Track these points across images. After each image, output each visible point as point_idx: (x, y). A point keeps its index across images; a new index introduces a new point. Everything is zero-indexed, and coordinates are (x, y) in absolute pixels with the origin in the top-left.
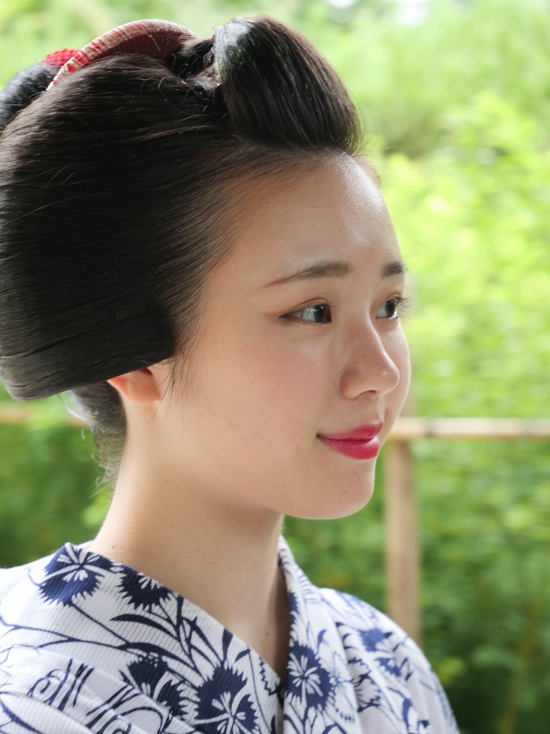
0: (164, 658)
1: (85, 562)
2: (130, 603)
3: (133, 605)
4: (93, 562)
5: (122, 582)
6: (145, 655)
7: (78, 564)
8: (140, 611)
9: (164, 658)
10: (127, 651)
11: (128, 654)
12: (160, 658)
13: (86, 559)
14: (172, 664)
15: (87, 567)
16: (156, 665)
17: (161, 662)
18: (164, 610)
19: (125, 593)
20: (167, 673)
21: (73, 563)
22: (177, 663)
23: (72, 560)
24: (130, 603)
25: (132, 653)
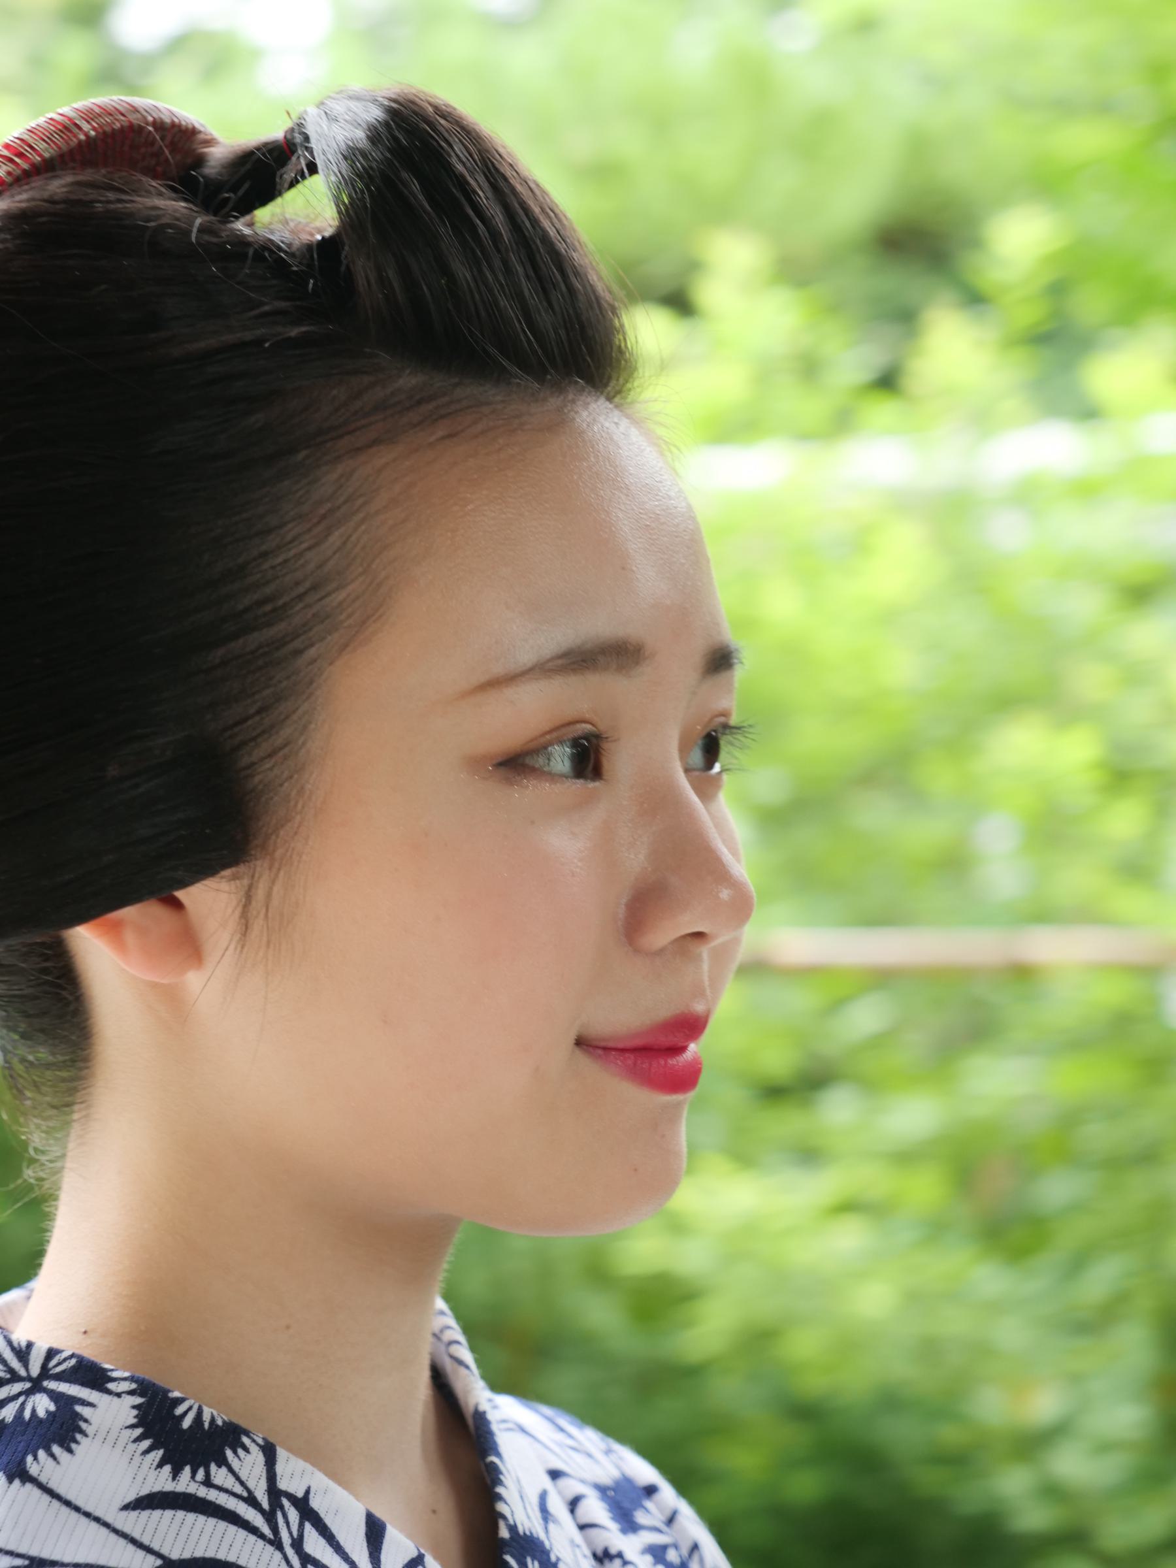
1: (45, 1373)
2: (160, 1465)
3: (167, 1468)
4: (64, 1371)
5: (136, 1417)
7: (29, 1378)
8: (186, 1483)
13: (44, 1367)
15: (52, 1385)
18: (238, 1478)
19: (146, 1443)
21: (15, 1377)
23: (11, 1371)
24: (160, 1465)
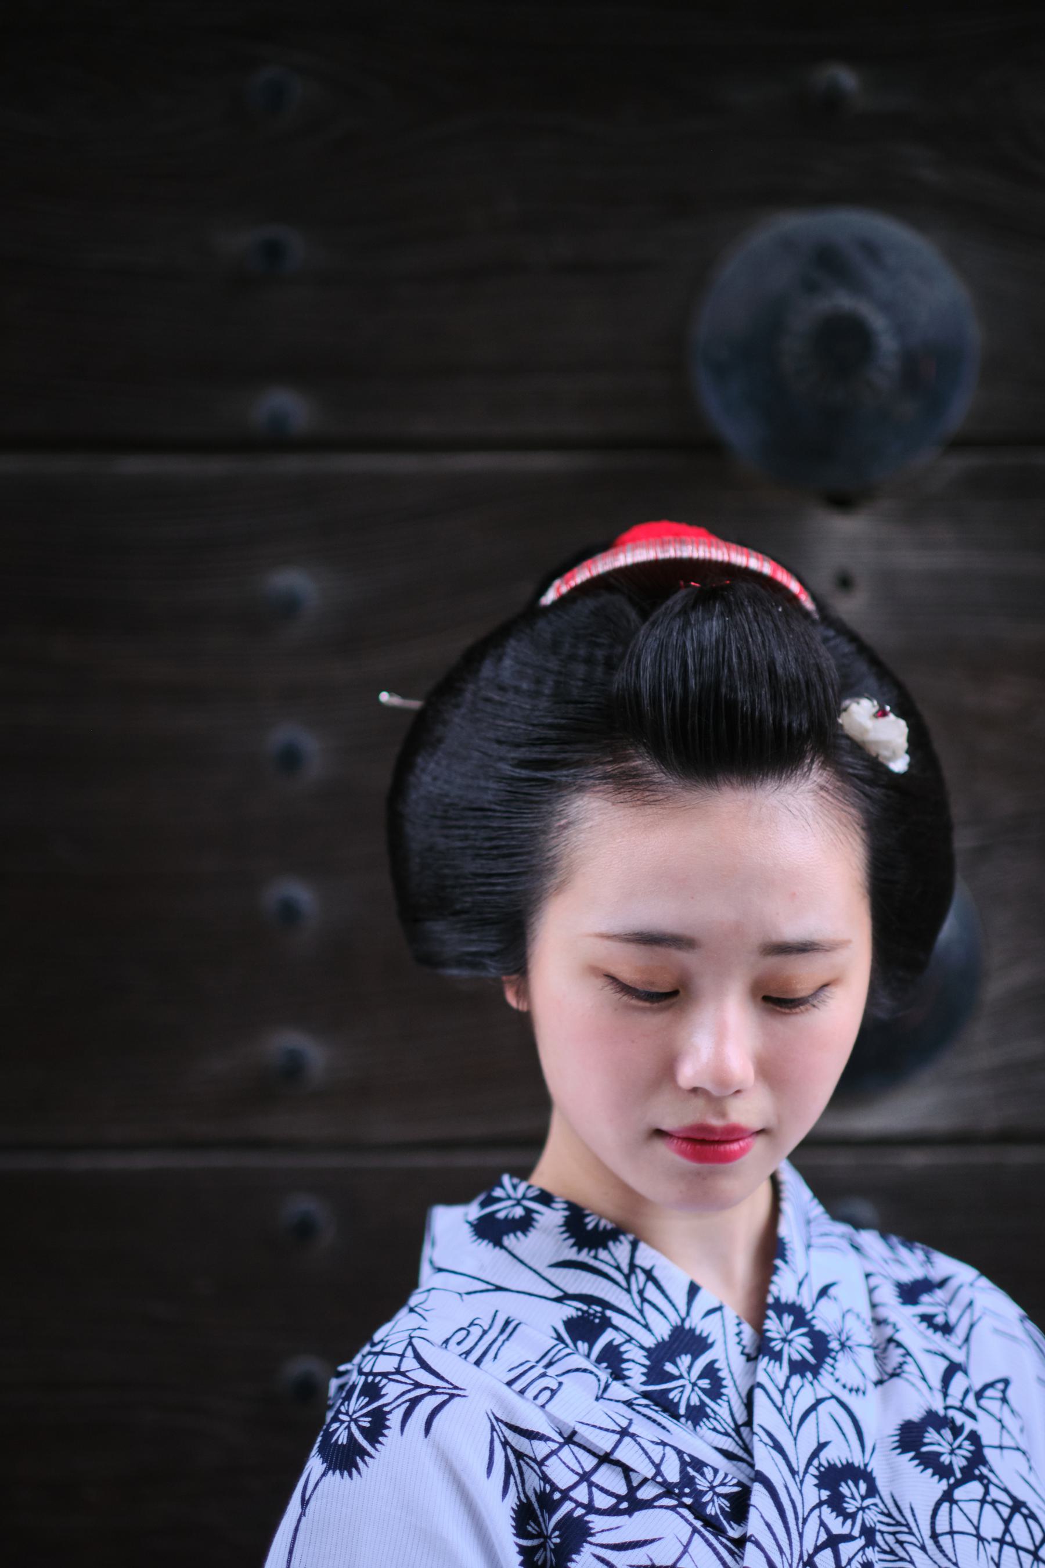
0: (609, 1313)
6: (585, 1308)
9: (609, 1313)
10: (564, 1304)
11: (565, 1307)
12: (603, 1313)
14: (616, 1319)
16: (597, 1321)
22: (624, 1318)
25: (569, 1306)
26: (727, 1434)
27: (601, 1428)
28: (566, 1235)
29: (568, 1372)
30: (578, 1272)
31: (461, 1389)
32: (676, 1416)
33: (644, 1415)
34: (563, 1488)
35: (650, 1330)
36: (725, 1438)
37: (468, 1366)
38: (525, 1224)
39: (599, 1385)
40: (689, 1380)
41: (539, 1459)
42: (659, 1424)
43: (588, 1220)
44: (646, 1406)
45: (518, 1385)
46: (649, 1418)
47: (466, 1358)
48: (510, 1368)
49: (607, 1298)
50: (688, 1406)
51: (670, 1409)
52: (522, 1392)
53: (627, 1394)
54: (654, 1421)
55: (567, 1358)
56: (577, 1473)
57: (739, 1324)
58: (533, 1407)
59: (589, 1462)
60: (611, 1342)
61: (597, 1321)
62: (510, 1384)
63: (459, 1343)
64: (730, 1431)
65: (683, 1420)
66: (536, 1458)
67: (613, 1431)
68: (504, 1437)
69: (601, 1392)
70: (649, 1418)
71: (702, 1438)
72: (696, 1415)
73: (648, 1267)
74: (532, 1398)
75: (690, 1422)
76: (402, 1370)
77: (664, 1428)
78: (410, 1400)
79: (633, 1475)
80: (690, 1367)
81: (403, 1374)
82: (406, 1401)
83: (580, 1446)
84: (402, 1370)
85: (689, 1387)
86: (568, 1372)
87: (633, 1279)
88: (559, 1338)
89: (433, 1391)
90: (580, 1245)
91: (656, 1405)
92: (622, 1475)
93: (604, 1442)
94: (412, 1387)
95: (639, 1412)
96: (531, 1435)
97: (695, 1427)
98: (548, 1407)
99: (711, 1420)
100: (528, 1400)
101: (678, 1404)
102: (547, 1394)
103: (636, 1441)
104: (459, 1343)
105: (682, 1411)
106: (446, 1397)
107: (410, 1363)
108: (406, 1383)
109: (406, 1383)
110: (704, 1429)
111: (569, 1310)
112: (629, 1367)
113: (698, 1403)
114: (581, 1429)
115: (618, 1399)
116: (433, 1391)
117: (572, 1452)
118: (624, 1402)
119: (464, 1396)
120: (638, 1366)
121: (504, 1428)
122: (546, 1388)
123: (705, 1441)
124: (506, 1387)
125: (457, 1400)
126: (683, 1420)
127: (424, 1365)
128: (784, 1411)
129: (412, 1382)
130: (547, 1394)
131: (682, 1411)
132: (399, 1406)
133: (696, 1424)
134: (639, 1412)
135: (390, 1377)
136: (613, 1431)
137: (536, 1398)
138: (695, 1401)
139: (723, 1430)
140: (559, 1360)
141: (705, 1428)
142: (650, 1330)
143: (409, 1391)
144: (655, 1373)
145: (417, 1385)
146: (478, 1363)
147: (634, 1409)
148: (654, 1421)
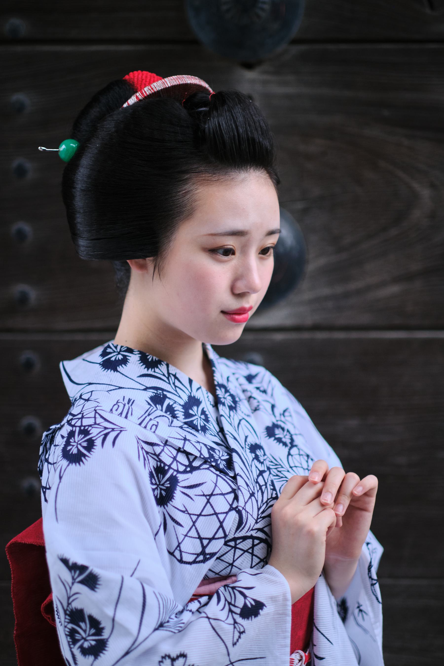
0: (165, 393)
12: (163, 393)
14: (169, 395)
17: (163, 395)
20: (167, 399)
26: (215, 436)
27: (177, 439)
28: (142, 364)
29: (156, 417)
30: (149, 378)
31: (124, 428)
32: (197, 431)
33: (187, 431)
34: (168, 465)
35: (181, 398)
36: (215, 437)
37: (122, 418)
38: (124, 361)
39: (169, 421)
40: (198, 416)
41: (157, 453)
42: (193, 434)
43: (148, 357)
44: (187, 427)
45: (144, 424)
46: (189, 432)
47: (121, 416)
48: (138, 418)
49: (163, 387)
50: (201, 426)
51: (195, 427)
52: (145, 427)
53: (181, 424)
54: (191, 433)
55: (155, 412)
56: (172, 457)
57: (207, 393)
58: (151, 432)
59: (175, 452)
60: (169, 404)
61: (162, 396)
62: (140, 424)
63: (116, 410)
64: (216, 435)
65: (200, 432)
66: (155, 453)
67: (181, 439)
68: (142, 446)
69: (170, 424)
70: (189, 432)
71: (208, 438)
72: (204, 429)
73: (174, 374)
74: (150, 430)
75: (203, 432)
76: (97, 423)
77: (195, 435)
78: (104, 434)
79: (190, 456)
80: (197, 411)
81: (98, 424)
82: (102, 435)
83: (170, 446)
84: (97, 423)
85: (199, 419)
86: (156, 417)
87: (170, 378)
88: (149, 404)
89: (113, 430)
90: (148, 367)
91: (190, 426)
92: (186, 457)
93: (180, 444)
94: (103, 429)
95: (185, 430)
96: (152, 444)
97: (205, 434)
98: (156, 432)
99: (209, 431)
100: (148, 430)
101: (197, 426)
102: (154, 427)
103: (190, 442)
104: (116, 410)
105: (199, 428)
106: (119, 432)
107: (99, 420)
108: (100, 428)
109: (100, 428)
110: (208, 435)
111: (150, 393)
112: (178, 413)
113: (203, 425)
114: (170, 440)
115: (177, 426)
116: (113, 430)
117: (168, 449)
118: (179, 427)
119: (126, 430)
120: (180, 412)
121: (141, 442)
122: (153, 425)
123: (209, 439)
124: (139, 426)
125: (123, 432)
126: (200, 432)
127: (106, 420)
128: (232, 425)
129: (103, 427)
130: (154, 427)
131: (199, 428)
132: (99, 437)
133: (205, 432)
134: (185, 430)
135: (92, 426)
136: (181, 439)
137: (151, 429)
138: (202, 424)
139: (214, 435)
140: (152, 413)
141: (208, 434)
142: (181, 398)
143: (103, 431)
144: (187, 415)
145: (106, 428)
146: (126, 417)
147: (183, 429)
148: (191, 433)
